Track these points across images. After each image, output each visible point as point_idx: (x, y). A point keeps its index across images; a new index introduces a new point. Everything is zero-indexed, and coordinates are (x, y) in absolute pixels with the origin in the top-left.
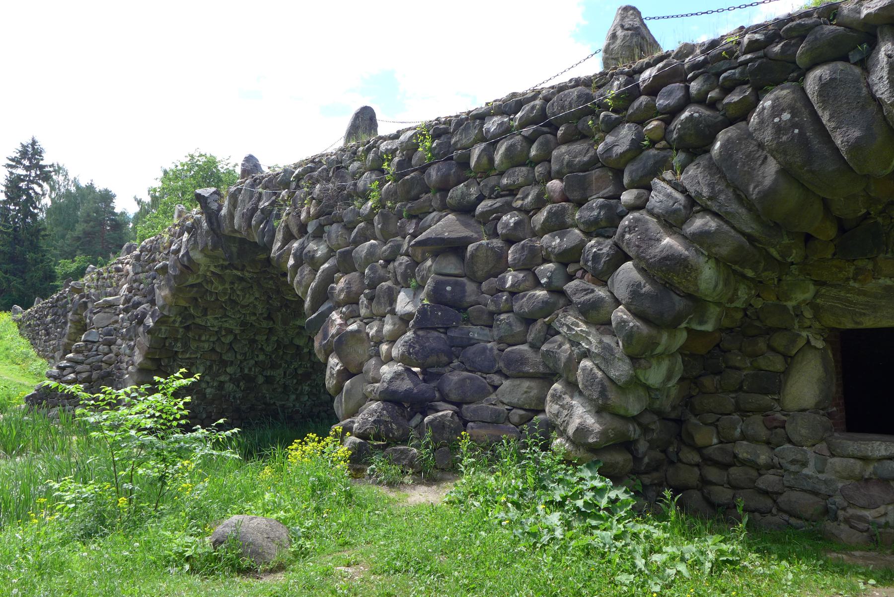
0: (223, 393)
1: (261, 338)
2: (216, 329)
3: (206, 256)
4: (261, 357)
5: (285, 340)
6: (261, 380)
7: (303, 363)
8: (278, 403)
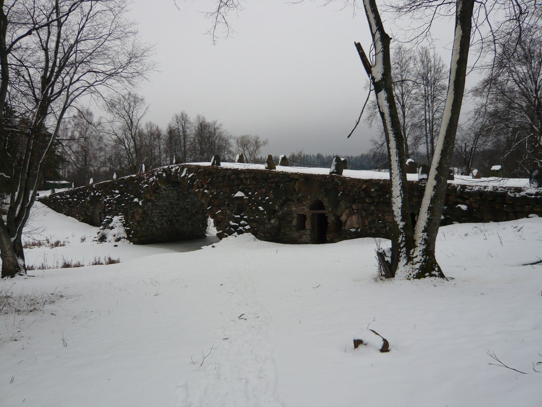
1: (175, 207)
4: (175, 213)
6: (175, 221)
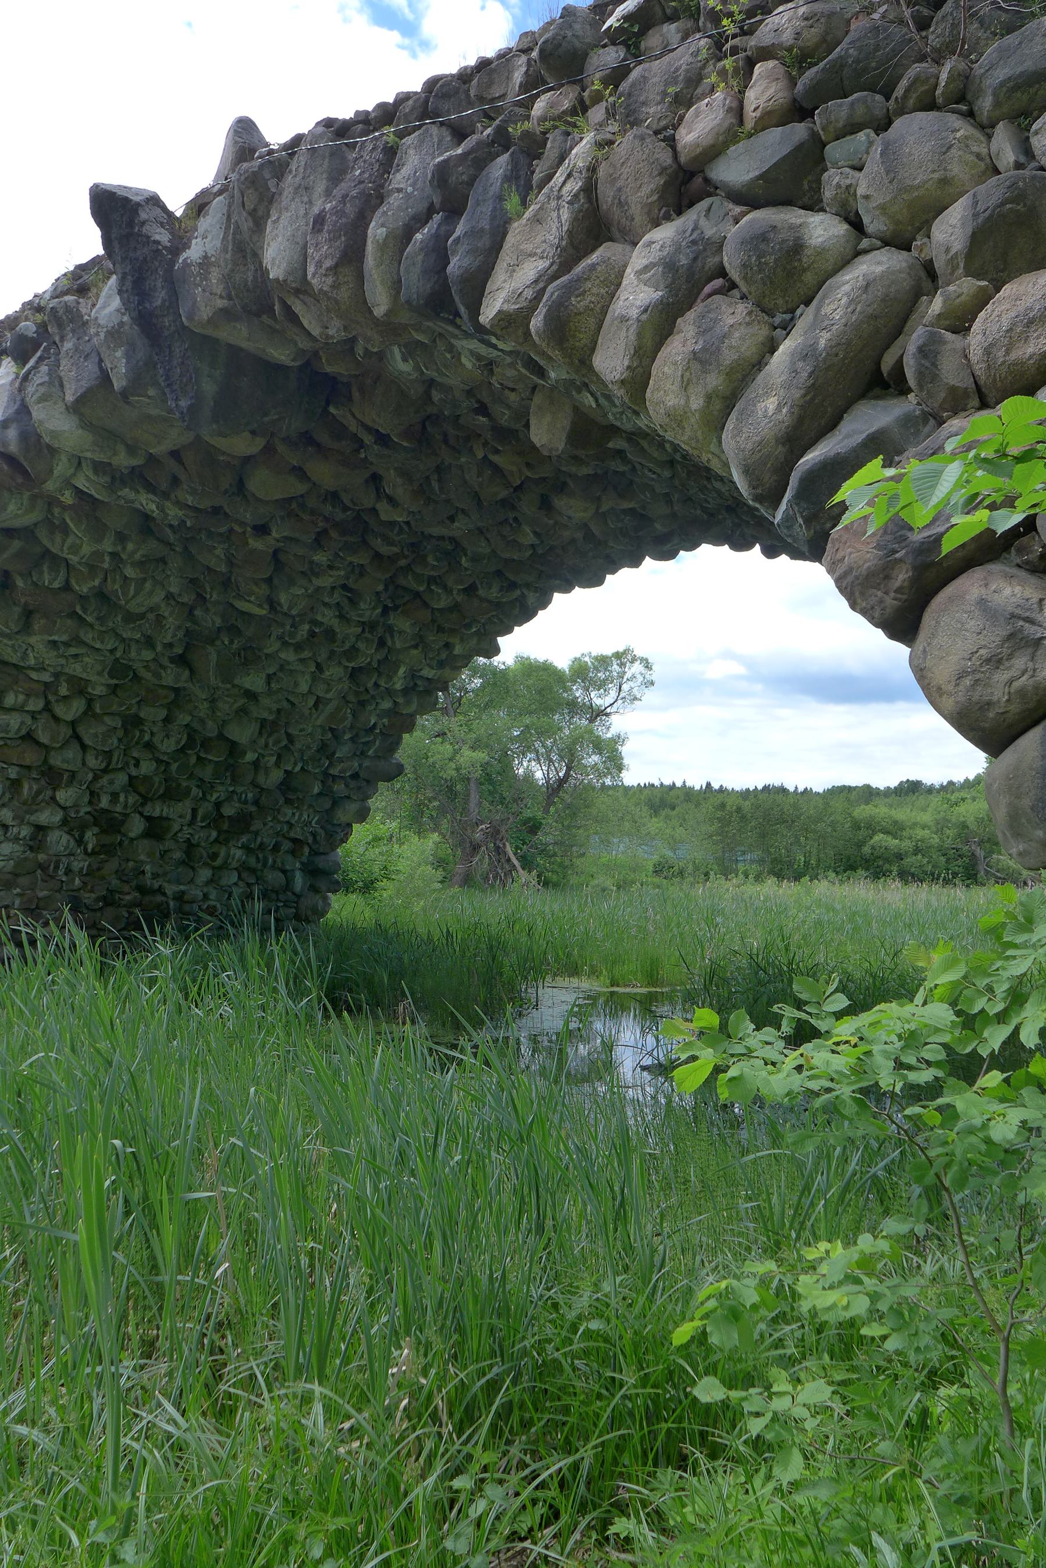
0: (42, 857)
1: (153, 714)
2: (46, 677)
3: (86, 424)
4: (147, 767)
5: (210, 724)
6: (136, 826)
7: (240, 789)
8: (171, 889)
